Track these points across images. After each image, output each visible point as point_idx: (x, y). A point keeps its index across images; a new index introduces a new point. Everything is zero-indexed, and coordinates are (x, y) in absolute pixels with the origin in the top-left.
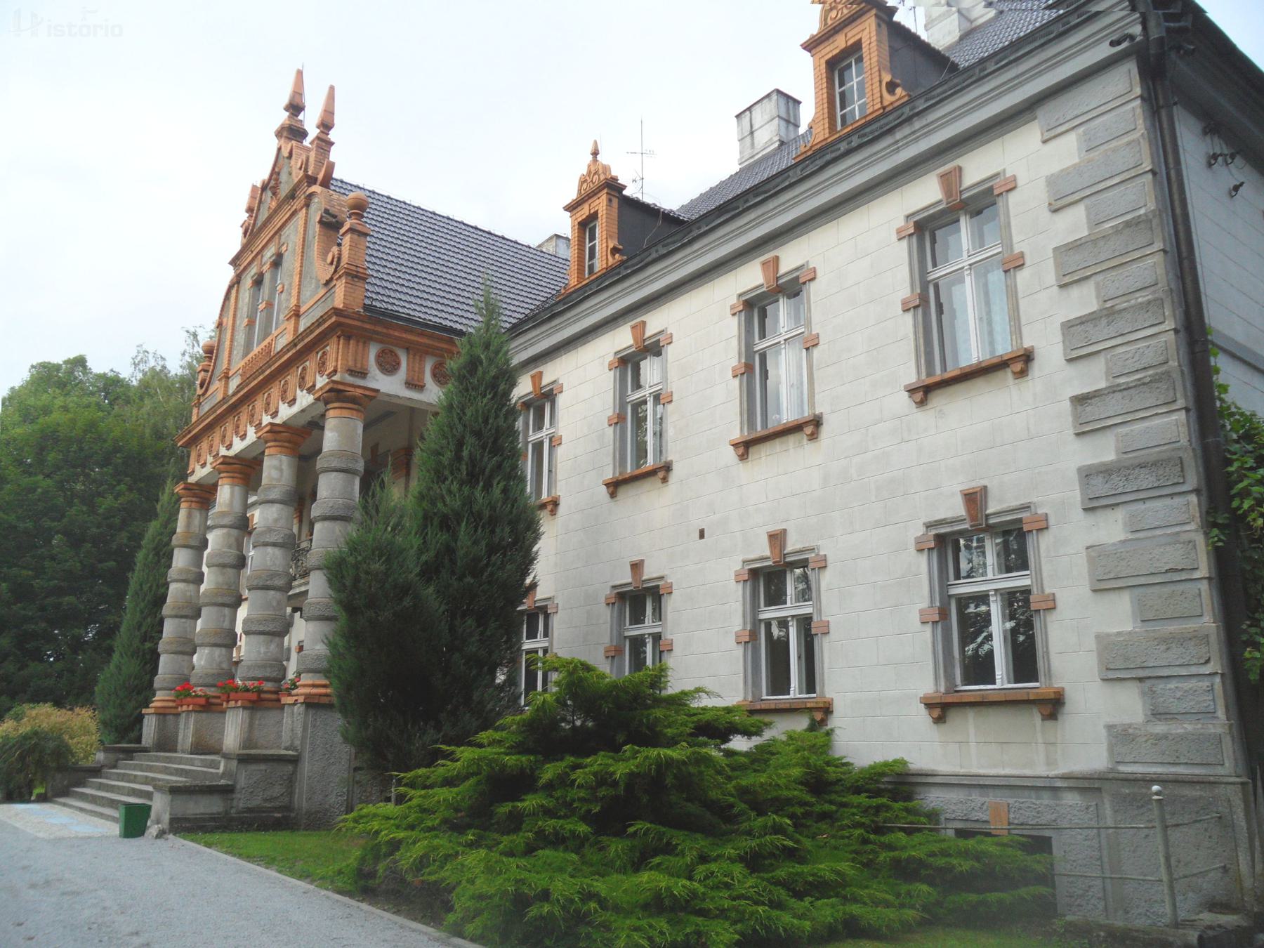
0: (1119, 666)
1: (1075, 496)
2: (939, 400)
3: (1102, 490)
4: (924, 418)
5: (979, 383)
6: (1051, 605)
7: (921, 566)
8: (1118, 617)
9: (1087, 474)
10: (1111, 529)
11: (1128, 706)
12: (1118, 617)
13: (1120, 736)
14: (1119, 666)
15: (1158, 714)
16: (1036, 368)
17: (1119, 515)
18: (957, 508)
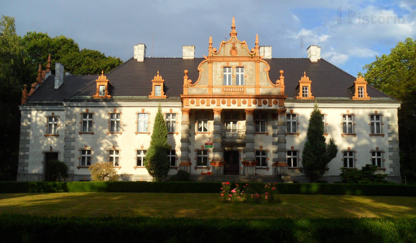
0: (391, 166)
1: (388, 150)
2: (373, 136)
3: (391, 150)
4: (370, 138)
5: (378, 136)
6: (384, 160)
7: (371, 154)
8: (391, 162)
9: (390, 148)
10: (391, 154)
11: (392, 170)
12: (391, 162)
13: (391, 173)
14: (391, 166)
15: (394, 171)
16: (385, 136)
17: (392, 153)
18: (375, 149)
